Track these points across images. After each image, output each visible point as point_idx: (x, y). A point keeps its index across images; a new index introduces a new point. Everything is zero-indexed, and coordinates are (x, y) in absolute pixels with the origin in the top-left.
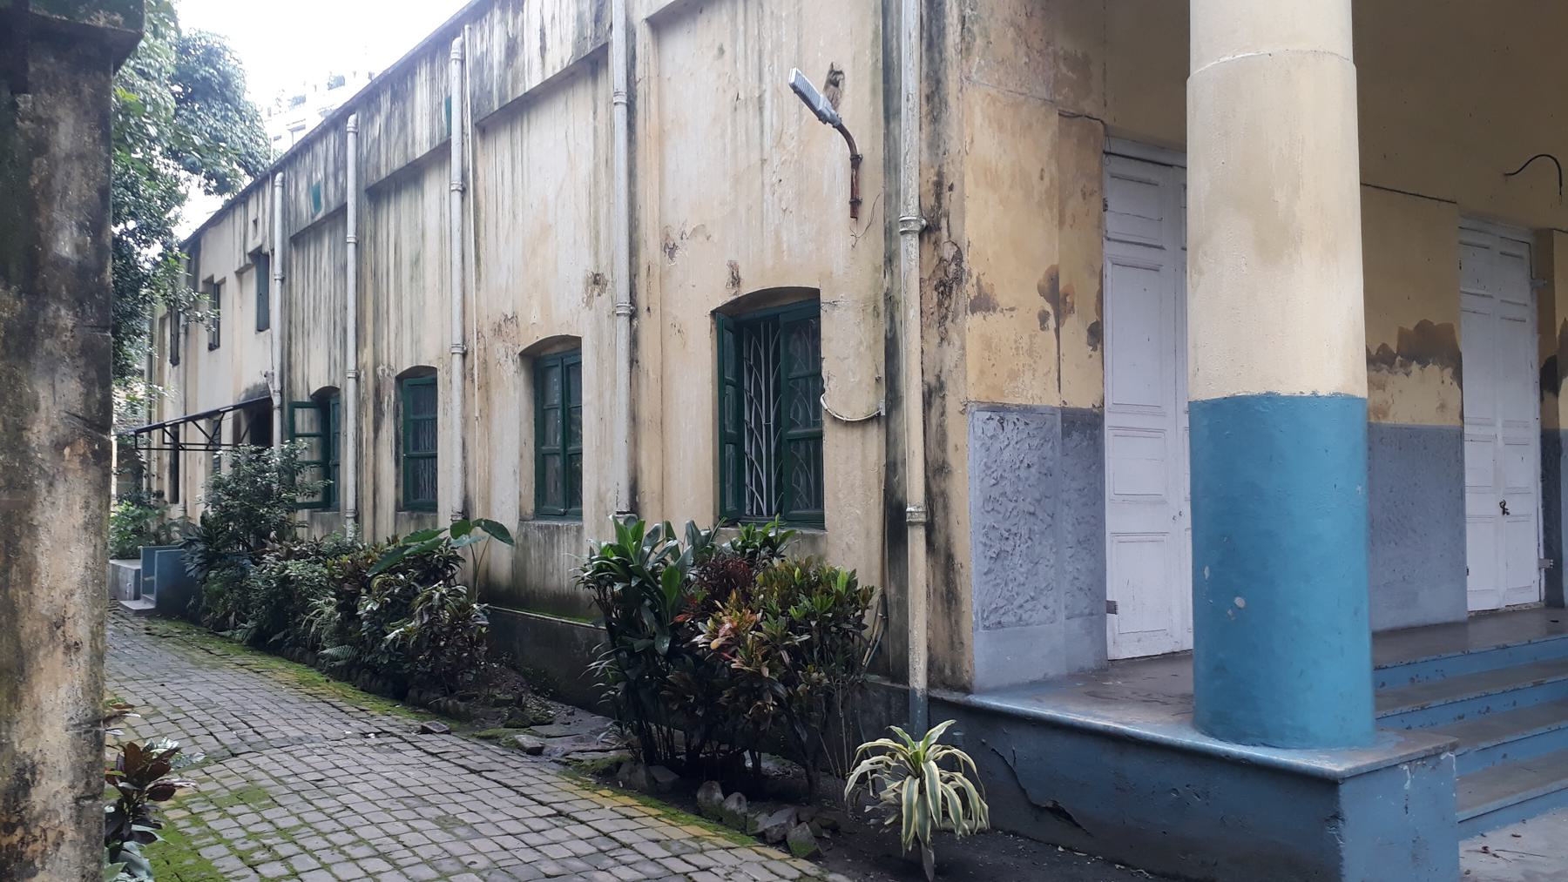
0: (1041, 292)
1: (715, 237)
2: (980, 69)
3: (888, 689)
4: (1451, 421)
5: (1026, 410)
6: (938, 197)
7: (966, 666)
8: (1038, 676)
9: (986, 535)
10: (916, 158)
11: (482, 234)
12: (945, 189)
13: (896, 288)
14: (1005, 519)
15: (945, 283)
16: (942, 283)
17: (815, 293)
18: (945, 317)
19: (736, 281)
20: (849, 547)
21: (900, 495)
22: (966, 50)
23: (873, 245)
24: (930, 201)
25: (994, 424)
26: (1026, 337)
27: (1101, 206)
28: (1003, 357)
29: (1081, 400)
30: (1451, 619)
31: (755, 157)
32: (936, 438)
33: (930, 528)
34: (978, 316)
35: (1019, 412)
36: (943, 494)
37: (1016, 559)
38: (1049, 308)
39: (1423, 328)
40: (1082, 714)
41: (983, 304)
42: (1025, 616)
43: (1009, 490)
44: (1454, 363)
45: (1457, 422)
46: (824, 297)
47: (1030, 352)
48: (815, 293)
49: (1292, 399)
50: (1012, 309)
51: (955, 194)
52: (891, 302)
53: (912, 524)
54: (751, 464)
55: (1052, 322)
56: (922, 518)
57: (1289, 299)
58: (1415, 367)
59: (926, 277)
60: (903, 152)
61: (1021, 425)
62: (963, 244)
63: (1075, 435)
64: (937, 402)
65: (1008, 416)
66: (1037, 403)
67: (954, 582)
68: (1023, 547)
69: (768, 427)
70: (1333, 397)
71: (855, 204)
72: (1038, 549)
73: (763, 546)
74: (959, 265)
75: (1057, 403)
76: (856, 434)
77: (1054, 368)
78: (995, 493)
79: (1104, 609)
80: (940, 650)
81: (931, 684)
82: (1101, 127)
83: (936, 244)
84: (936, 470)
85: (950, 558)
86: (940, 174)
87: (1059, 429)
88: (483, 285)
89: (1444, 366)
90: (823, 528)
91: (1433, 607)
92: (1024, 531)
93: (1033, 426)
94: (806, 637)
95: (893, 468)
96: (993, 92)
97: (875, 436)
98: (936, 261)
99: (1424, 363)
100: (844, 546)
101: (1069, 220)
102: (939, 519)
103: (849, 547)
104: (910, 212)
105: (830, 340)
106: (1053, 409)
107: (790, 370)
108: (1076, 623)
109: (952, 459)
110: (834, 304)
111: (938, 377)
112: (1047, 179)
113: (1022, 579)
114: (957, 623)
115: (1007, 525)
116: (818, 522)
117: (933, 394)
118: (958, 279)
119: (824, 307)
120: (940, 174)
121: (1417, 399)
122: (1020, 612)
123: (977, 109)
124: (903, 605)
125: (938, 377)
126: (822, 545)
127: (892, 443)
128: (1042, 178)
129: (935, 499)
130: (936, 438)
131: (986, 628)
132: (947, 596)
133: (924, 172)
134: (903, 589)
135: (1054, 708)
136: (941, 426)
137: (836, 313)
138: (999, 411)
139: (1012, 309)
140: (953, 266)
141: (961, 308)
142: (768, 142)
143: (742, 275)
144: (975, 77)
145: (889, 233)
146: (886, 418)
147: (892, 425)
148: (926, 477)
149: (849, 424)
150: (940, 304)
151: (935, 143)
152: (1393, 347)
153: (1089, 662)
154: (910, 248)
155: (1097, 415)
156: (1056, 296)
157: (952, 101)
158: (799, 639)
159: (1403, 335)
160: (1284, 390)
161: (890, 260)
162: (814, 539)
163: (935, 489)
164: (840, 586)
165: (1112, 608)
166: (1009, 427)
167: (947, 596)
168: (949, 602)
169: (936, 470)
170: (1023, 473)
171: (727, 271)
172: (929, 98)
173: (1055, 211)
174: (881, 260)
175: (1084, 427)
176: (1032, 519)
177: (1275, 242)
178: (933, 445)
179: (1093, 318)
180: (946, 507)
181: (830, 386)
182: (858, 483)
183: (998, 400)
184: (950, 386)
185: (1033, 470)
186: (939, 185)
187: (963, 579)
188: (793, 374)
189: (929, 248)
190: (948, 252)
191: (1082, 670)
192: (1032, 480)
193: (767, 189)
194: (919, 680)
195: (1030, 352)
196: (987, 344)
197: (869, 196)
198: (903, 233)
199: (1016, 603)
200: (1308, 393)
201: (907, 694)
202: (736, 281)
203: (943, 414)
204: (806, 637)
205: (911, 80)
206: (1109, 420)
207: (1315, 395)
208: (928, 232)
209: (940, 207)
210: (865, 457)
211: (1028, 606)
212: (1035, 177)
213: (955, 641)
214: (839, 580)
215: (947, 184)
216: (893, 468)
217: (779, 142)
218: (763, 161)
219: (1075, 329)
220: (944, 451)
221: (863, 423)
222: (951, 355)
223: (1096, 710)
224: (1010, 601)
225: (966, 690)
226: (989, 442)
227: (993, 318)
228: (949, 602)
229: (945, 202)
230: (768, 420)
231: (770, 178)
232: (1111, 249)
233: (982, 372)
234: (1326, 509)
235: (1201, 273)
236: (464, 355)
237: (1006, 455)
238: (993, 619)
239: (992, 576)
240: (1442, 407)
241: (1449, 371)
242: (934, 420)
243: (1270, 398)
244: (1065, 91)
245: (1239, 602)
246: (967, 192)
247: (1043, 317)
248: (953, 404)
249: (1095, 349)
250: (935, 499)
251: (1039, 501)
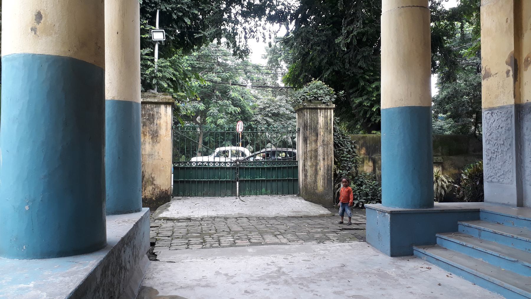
0: (507, 63)
5: (501, 108)
26: (501, 82)
35: (499, 109)
42: (501, 180)
43: (494, 136)
47: (503, 87)
50: (496, 74)
61: (499, 114)
66: (505, 104)
72: (505, 157)
112: (509, 21)
113: (500, 167)
122: (499, 178)
128: (507, 22)
139: (496, 74)
166: (494, 115)
170: (500, 130)
176: (503, 146)
183: (491, 106)
185: (503, 129)
192: (503, 132)
195: (503, 87)
211: (502, 177)
237: (493, 125)
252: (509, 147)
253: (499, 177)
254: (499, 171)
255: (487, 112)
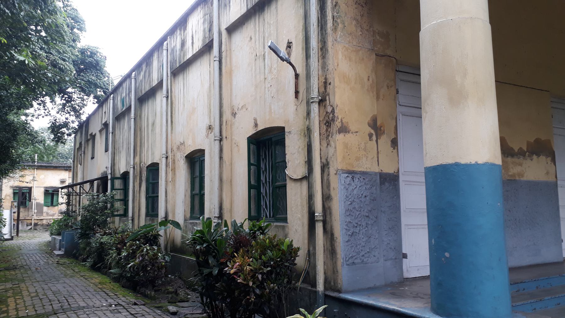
0: (369, 125)
1: (249, 109)
2: (341, 37)
3: (310, 290)
4: (551, 179)
5: (364, 173)
6: (325, 88)
7: (339, 281)
8: (372, 285)
9: (347, 225)
10: (316, 73)
11: (174, 113)
12: (328, 84)
13: (312, 124)
14: (356, 218)
15: (328, 122)
16: (327, 122)
17: (283, 128)
18: (329, 135)
19: (256, 125)
20: (296, 231)
21: (313, 208)
22: (335, 29)
23: (303, 108)
24: (322, 90)
25: (349, 179)
26: (363, 144)
27: (395, 92)
28: (351, 151)
29: (389, 169)
30: (556, 261)
31: (262, 77)
32: (326, 185)
33: (324, 222)
34: (342, 135)
36: (330, 208)
37: (361, 236)
38: (373, 132)
39: (537, 141)
40: (384, 303)
41: (344, 130)
42: (365, 260)
43: (357, 206)
44: (552, 155)
45: (554, 179)
46: (286, 130)
47: (365, 150)
48: (283, 128)
49: (467, 166)
50: (357, 132)
51: (331, 86)
52: (309, 131)
53: (317, 221)
54: (263, 197)
55: (374, 138)
56: (321, 218)
57: (464, 122)
58: (535, 157)
59: (321, 119)
60: (311, 70)
61: (361, 179)
62: (335, 106)
63: (387, 184)
64: (326, 170)
65: (356, 176)
66: (368, 170)
67: (334, 245)
68: (364, 230)
69: (269, 182)
70: (485, 164)
71: (297, 93)
72: (370, 232)
73: (258, 230)
74: (333, 114)
75: (377, 170)
76: (298, 184)
77: (376, 156)
78: (351, 207)
79: (402, 256)
80: (329, 274)
81: (326, 288)
82: (395, 60)
83: (325, 106)
84: (327, 198)
85: (332, 235)
86: (326, 79)
87: (378, 181)
88: (174, 131)
89: (547, 156)
90: (287, 222)
91: (547, 256)
92: (364, 224)
93: (367, 180)
94: (269, 269)
95: (311, 197)
96: (347, 46)
97: (305, 184)
98: (325, 113)
99: (538, 155)
100: (294, 230)
101: (381, 97)
102: (328, 219)
103: (296, 231)
104: (315, 93)
105: (289, 147)
106: (376, 173)
107: (275, 159)
108: (389, 263)
109: (333, 193)
110: (290, 132)
111: (327, 160)
112: (371, 80)
113: (363, 244)
114: (336, 262)
115: (356, 221)
116: (285, 220)
117: (325, 167)
118: (333, 120)
119: (286, 134)
120: (326, 79)
121: (533, 170)
122: (363, 258)
123: (340, 53)
124: (314, 254)
125: (327, 160)
126: (287, 229)
127: (310, 188)
128: (368, 80)
129: (326, 210)
130: (326, 185)
131: (347, 265)
132: (331, 251)
133: (320, 78)
134: (314, 248)
135: (373, 300)
136: (328, 180)
137: (291, 136)
138: (351, 173)
139: (357, 132)
140: (331, 115)
141: (334, 132)
142: (267, 71)
143: (258, 123)
144: (339, 40)
145: (308, 104)
146: (307, 178)
147: (310, 180)
148: (323, 201)
149: (296, 180)
150: (327, 130)
151: (324, 67)
152: (525, 149)
153: (395, 279)
154: (315, 108)
155: (396, 176)
156: (376, 128)
157: (330, 49)
158: (265, 270)
159: (528, 144)
160: (463, 162)
161: (308, 114)
162: (283, 228)
163: (326, 206)
164: (284, 247)
165: (405, 256)
166: (356, 180)
167: (331, 251)
168: (332, 254)
169: (327, 198)
170: (363, 199)
171: (253, 121)
172: (321, 49)
173: (375, 93)
174: (306, 114)
175: (390, 181)
177: (457, 98)
178: (325, 187)
179: (393, 136)
180: (330, 213)
181: (289, 165)
182: (299, 204)
183: (351, 169)
184: (331, 163)
185: (368, 198)
186: (325, 83)
187: (337, 244)
188: (277, 161)
189: (322, 108)
190: (329, 109)
191: (392, 283)
193: (267, 89)
194: (320, 287)
195: (365, 150)
196: (346, 146)
197: (302, 89)
198: (312, 102)
199: (361, 254)
200: (473, 162)
201: (316, 292)
202: (256, 125)
203: (329, 175)
204: (269, 269)
205: (314, 43)
206: (401, 178)
207: (477, 164)
208: (322, 102)
209: (326, 92)
210: (301, 193)
211: (366, 256)
212: (366, 80)
213: (335, 271)
214: (285, 244)
215: (328, 82)
216: (311, 197)
217: (270, 71)
218: (265, 79)
219: (385, 141)
220: (329, 190)
221: (301, 180)
222: (331, 150)
223: (392, 302)
224: (358, 253)
225: (339, 291)
226: (347, 186)
227: (348, 136)
228: (332, 254)
229: (328, 90)
230: (269, 179)
231: (268, 85)
232: (400, 109)
233: (344, 157)
234: (485, 212)
235: (426, 113)
236: (167, 158)
237: (355, 192)
238: (351, 261)
239: (350, 243)
240: (548, 173)
241: (549, 159)
242: (325, 178)
243: (457, 165)
244: (379, 46)
245: (447, 255)
246: (336, 85)
247: (370, 136)
248: (332, 171)
249: (394, 149)
250: (326, 210)
251: (370, 211)
252: (375, 219)
253: (363, 256)
254: (363, 248)
255: (347, 175)
